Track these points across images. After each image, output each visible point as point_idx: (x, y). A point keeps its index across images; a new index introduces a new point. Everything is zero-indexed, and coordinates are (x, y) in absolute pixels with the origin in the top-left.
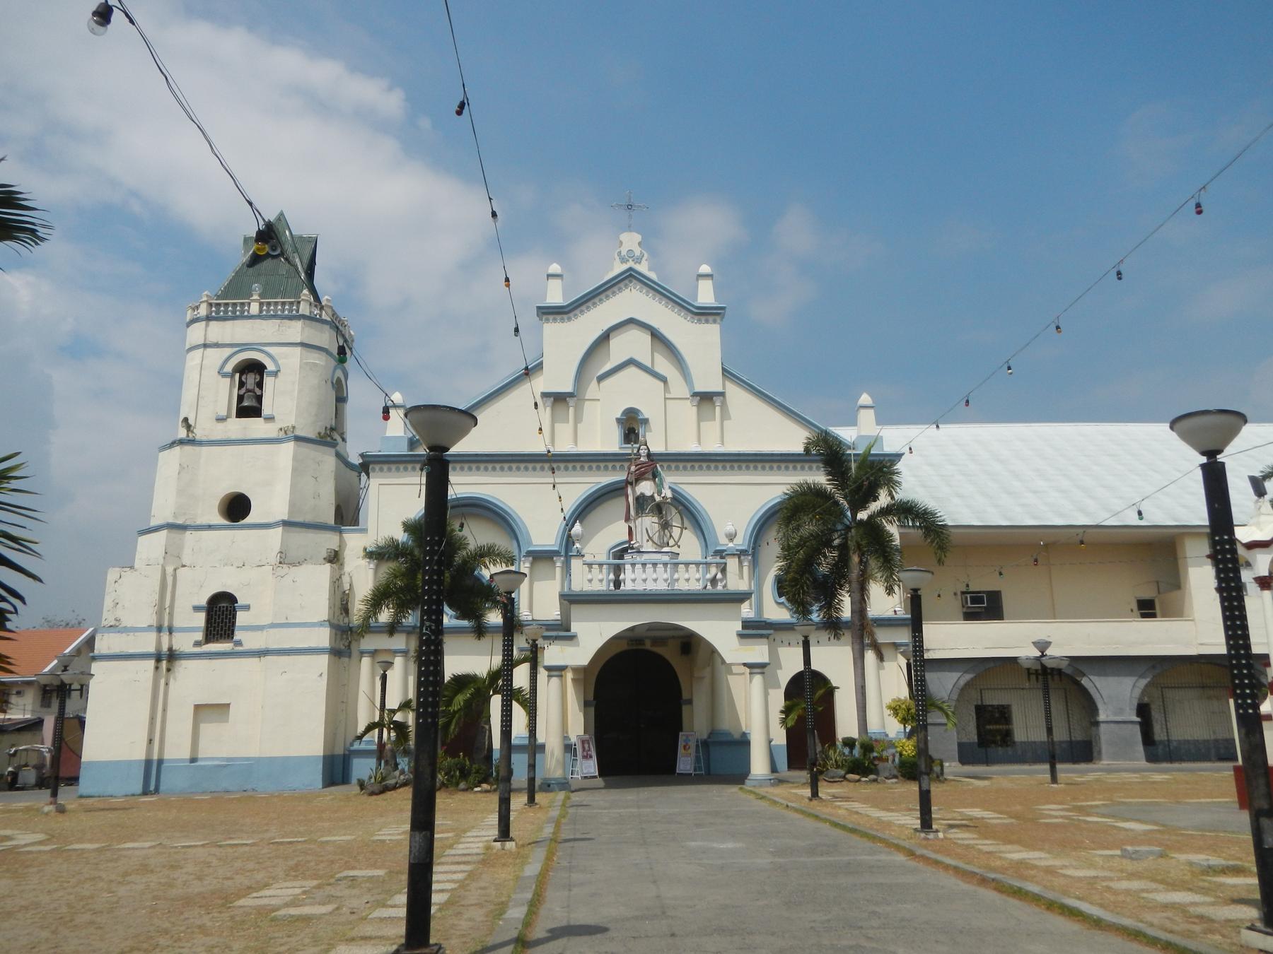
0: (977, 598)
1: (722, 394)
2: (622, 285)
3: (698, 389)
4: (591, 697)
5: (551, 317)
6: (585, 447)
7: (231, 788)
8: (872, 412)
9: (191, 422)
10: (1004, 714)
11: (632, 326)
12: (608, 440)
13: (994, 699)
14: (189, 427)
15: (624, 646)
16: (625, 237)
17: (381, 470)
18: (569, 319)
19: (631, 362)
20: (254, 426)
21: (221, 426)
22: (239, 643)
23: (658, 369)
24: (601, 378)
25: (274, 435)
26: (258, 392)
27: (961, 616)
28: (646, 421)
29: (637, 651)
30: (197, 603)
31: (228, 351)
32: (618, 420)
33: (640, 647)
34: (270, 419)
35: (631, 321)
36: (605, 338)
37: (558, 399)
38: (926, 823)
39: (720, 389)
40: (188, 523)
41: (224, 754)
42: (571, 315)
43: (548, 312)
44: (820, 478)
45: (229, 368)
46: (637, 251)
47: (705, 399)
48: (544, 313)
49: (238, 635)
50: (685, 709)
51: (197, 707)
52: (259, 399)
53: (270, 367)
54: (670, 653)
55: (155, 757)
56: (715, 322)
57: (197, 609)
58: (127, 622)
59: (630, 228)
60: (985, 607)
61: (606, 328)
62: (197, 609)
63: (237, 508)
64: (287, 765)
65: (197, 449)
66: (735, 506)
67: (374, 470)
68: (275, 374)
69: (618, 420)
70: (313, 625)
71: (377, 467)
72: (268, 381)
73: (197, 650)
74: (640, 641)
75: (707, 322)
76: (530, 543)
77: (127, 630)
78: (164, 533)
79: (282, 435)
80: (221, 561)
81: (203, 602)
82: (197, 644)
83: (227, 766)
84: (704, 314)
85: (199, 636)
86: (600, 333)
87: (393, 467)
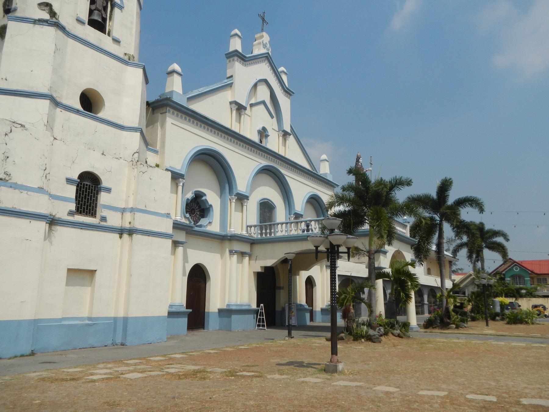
2: (263, 59)
5: (239, 60)
7: (96, 345)
8: (327, 163)
9: (56, 8)
11: (264, 83)
14: (53, 14)
16: (264, 34)
17: (173, 114)
18: (245, 66)
19: (263, 103)
21: (79, 26)
22: (104, 219)
24: (252, 105)
25: (121, 55)
26: (104, 16)
34: (117, 41)
35: (265, 81)
36: (255, 86)
37: (240, 108)
40: (58, 100)
41: (85, 314)
42: (246, 63)
43: (236, 54)
46: (268, 46)
47: (285, 134)
49: (101, 212)
51: (69, 270)
52: (104, 20)
56: (289, 98)
57: (69, 181)
58: (17, 178)
59: (262, 30)
62: (69, 181)
63: (89, 102)
64: (146, 322)
65: (66, 37)
68: (121, 8)
71: (172, 110)
73: (70, 218)
75: (287, 97)
76: (236, 188)
78: (46, 103)
79: (126, 58)
80: (85, 146)
81: (75, 177)
82: (71, 213)
83: (92, 324)
84: (288, 92)
85: (73, 206)
86: (254, 81)
87: (180, 114)
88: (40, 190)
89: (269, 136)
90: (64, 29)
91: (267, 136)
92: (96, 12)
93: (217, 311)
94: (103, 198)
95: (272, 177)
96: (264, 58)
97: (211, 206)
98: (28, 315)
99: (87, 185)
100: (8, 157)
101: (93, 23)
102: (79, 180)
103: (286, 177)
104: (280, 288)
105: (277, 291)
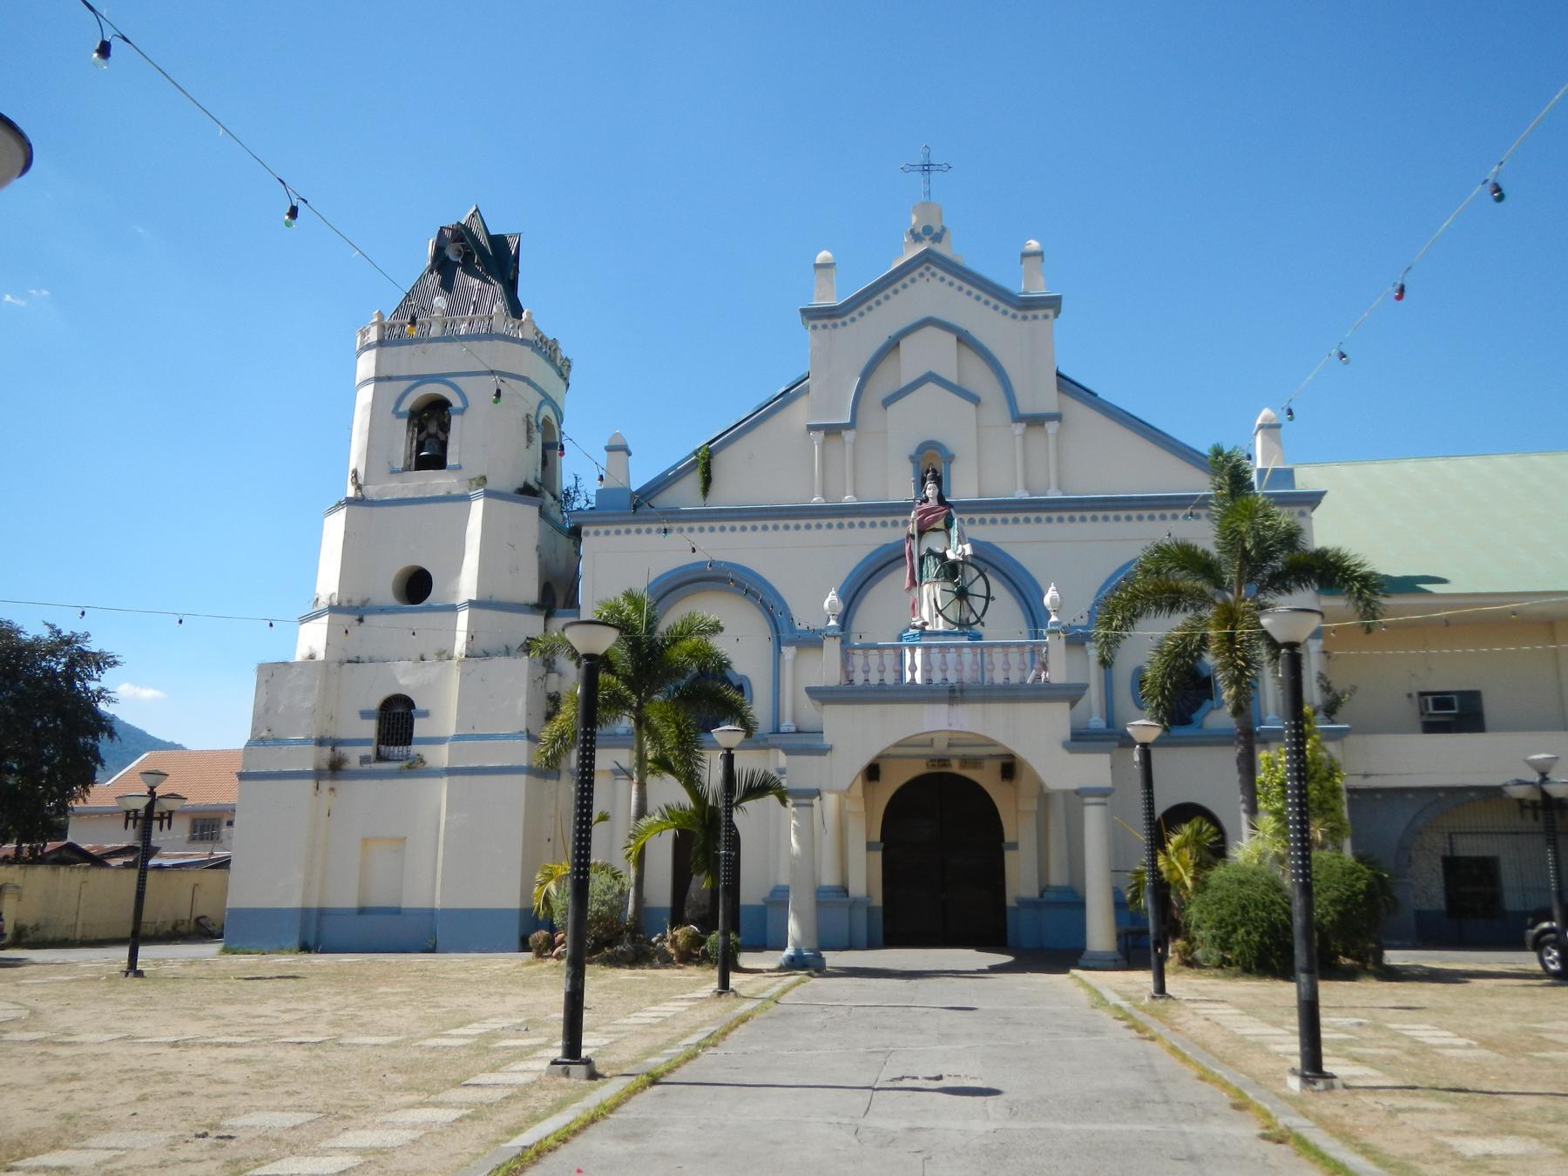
0: (1442, 700)
1: (1057, 417)
2: (915, 274)
3: (1025, 407)
4: (876, 837)
6: (872, 495)
10: (1487, 869)
12: (901, 487)
13: (1468, 848)
15: (919, 768)
19: (930, 377)
20: (436, 482)
23: (972, 387)
24: (887, 402)
27: (1419, 726)
28: (950, 458)
29: (940, 774)
30: (365, 708)
31: (405, 385)
32: (912, 458)
33: (943, 770)
35: (929, 322)
37: (832, 431)
38: (1312, 1064)
39: (1054, 410)
44: (1203, 535)
45: (406, 406)
47: (1035, 421)
48: (811, 318)
50: (1009, 856)
51: (365, 841)
52: (443, 446)
53: (456, 403)
54: (986, 778)
57: (365, 715)
60: (1455, 713)
61: (894, 330)
62: (365, 715)
66: (1073, 570)
67: (587, 534)
68: (461, 411)
69: (912, 458)
70: (507, 737)
71: (592, 529)
72: (455, 421)
74: (944, 761)
77: (278, 742)
81: (374, 704)
82: (364, 760)
85: (369, 750)
91: (950, 458)
94: (420, 728)
96: (922, 269)
98: (295, 902)
101: (422, 464)
103: (1004, 548)
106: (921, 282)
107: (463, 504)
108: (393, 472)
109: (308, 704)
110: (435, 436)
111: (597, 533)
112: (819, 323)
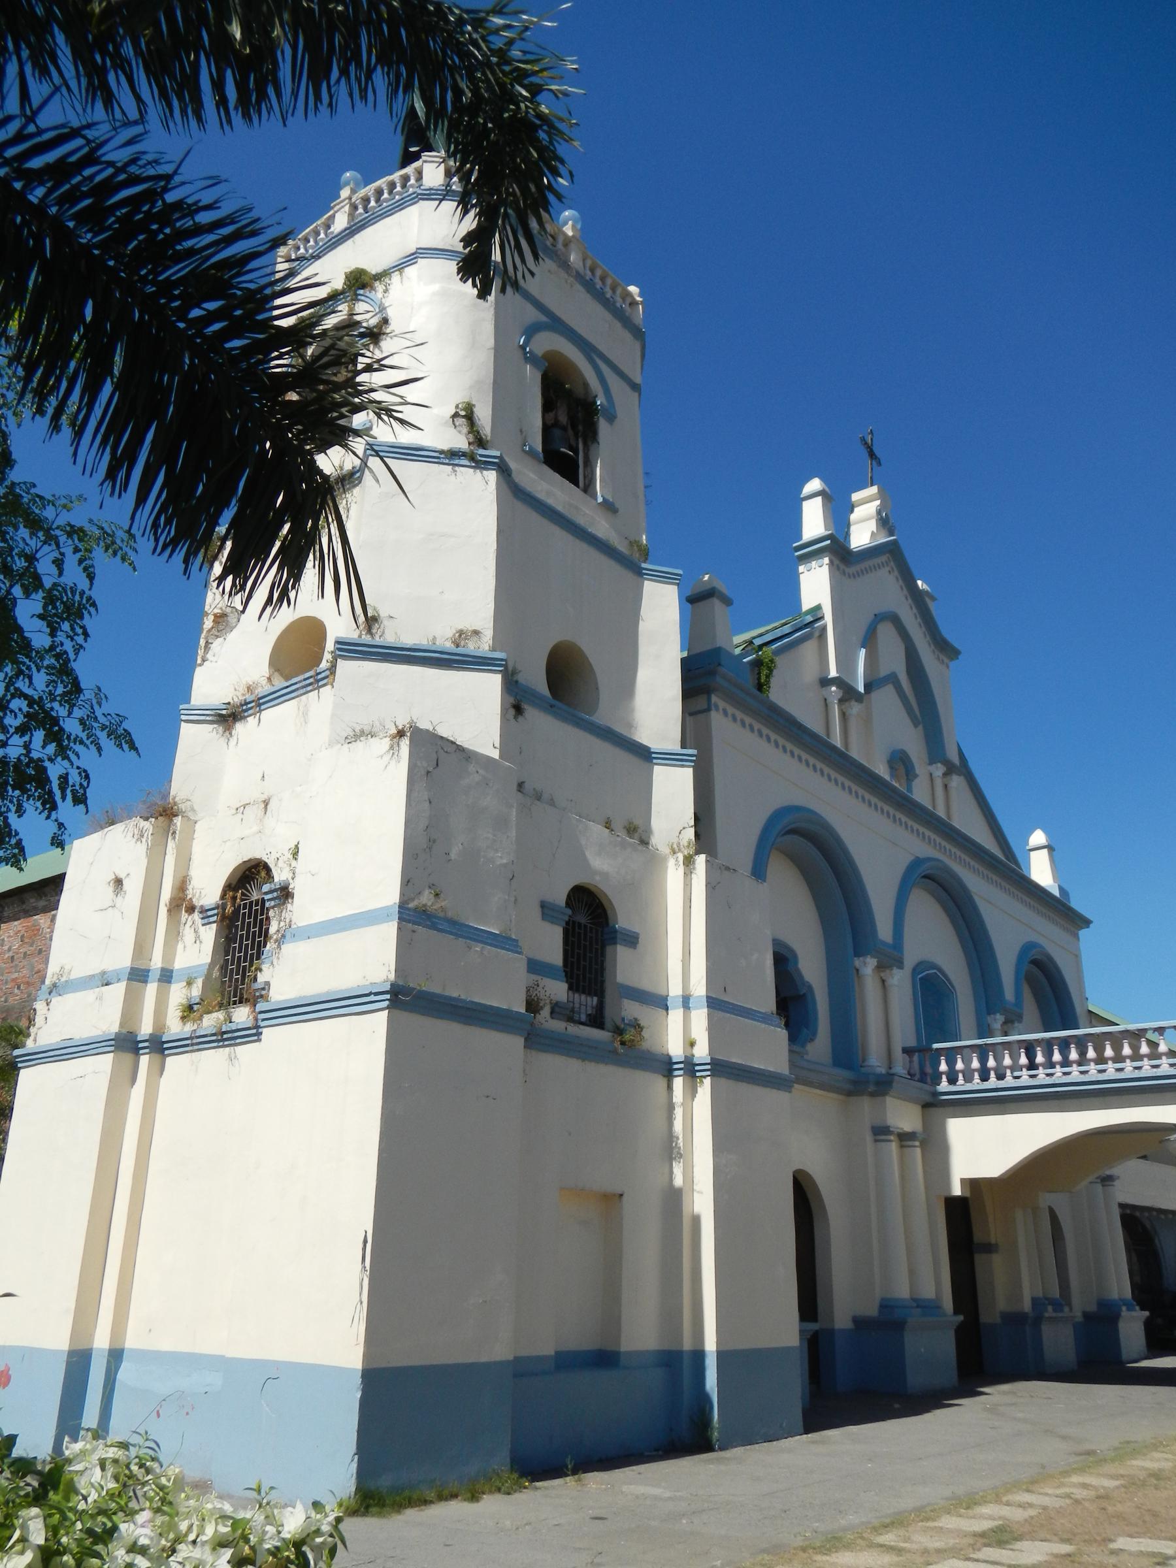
19: (892, 679)
30: (549, 898)
35: (895, 620)
42: (851, 570)
55: (101, 1341)
71: (722, 704)
72: (603, 425)
81: (560, 897)
82: (557, 1010)
88: (503, 942)
89: (916, 776)
90: (510, 475)
92: (557, 432)
93: (849, 1325)
94: (624, 966)
95: (939, 900)
96: (884, 558)
97: (810, 988)
99: (580, 924)
100: (434, 841)
102: (569, 912)
103: (976, 898)
104: (989, 1248)
105: (979, 1259)
106: (887, 569)
107: (629, 575)
108: (531, 453)
109: (502, 858)
110: (564, 429)
111: (725, 713)
112: (836, 562)
